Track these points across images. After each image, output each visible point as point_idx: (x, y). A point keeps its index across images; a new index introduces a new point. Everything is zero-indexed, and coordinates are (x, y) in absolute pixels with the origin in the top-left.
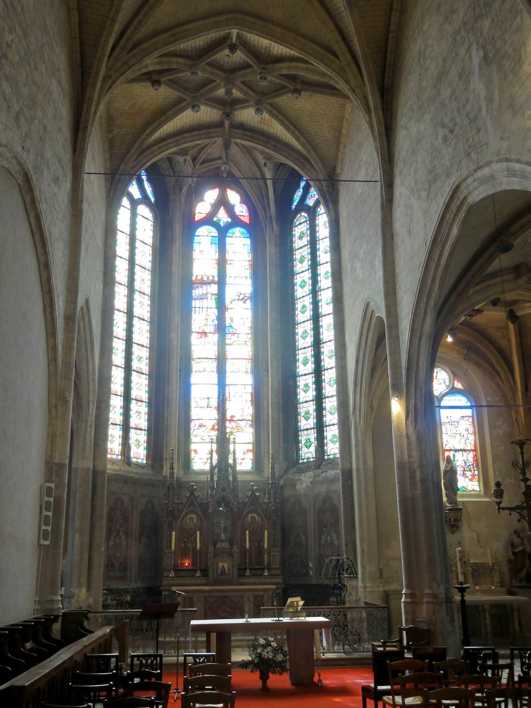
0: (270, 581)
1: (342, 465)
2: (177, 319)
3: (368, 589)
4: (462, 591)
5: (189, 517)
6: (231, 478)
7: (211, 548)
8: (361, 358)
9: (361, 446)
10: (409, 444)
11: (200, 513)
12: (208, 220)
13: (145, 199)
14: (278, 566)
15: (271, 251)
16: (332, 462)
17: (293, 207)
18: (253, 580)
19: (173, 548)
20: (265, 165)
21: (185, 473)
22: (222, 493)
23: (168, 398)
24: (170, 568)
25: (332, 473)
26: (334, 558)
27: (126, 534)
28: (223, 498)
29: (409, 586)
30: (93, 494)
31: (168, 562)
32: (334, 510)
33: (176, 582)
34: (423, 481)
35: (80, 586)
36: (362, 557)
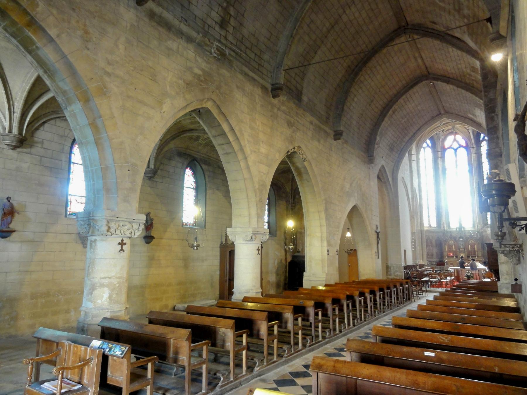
7: (458, 250)
13: (428, 146)
15: (474, 156)
17: (481, 139)
19: (446, 250)
27: (432, 247)
30: (422, 236)
31: (445, 254)
35: (420, 259)
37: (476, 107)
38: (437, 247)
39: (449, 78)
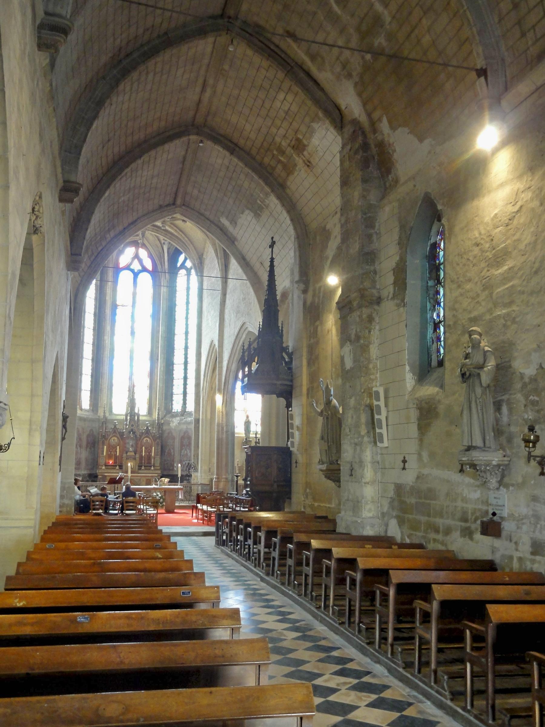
0: (154, 472)
1: (195, 416)
2: (108, 328)
3: (203, 477)
4: (237, 476)
5: (113, 438)
6: (136, 419)
8: (208, 364)
9: (205, 408)
10: (222, 416)
11: (119, 436)
12: (127, 268)
14: (158, 465)
15: (164, 290)
16: (190, 414)
17: (179, 265)
18: (146, 471)
19: (105, 454)
20: (164, 243)
21: (109, 415)
22: (132, 428)
23: (102, 373)
24: (102, 464)
25: (189, 419)
26: (187, 462)
28: (132, 430)
29: (217, 474)
31: (102, 461)
32: (189, 438)
33: (106, 471)
34: (227, 432)
36: (201, 462)
37: (248, 208)
38: (88, 449)
39: (236, 145)
